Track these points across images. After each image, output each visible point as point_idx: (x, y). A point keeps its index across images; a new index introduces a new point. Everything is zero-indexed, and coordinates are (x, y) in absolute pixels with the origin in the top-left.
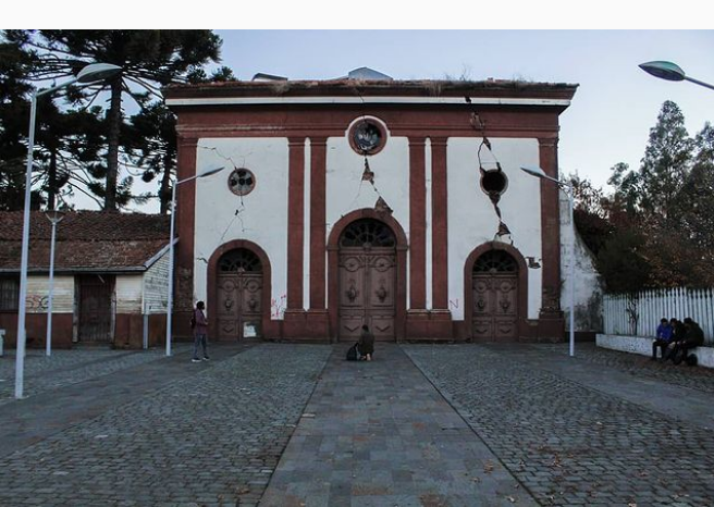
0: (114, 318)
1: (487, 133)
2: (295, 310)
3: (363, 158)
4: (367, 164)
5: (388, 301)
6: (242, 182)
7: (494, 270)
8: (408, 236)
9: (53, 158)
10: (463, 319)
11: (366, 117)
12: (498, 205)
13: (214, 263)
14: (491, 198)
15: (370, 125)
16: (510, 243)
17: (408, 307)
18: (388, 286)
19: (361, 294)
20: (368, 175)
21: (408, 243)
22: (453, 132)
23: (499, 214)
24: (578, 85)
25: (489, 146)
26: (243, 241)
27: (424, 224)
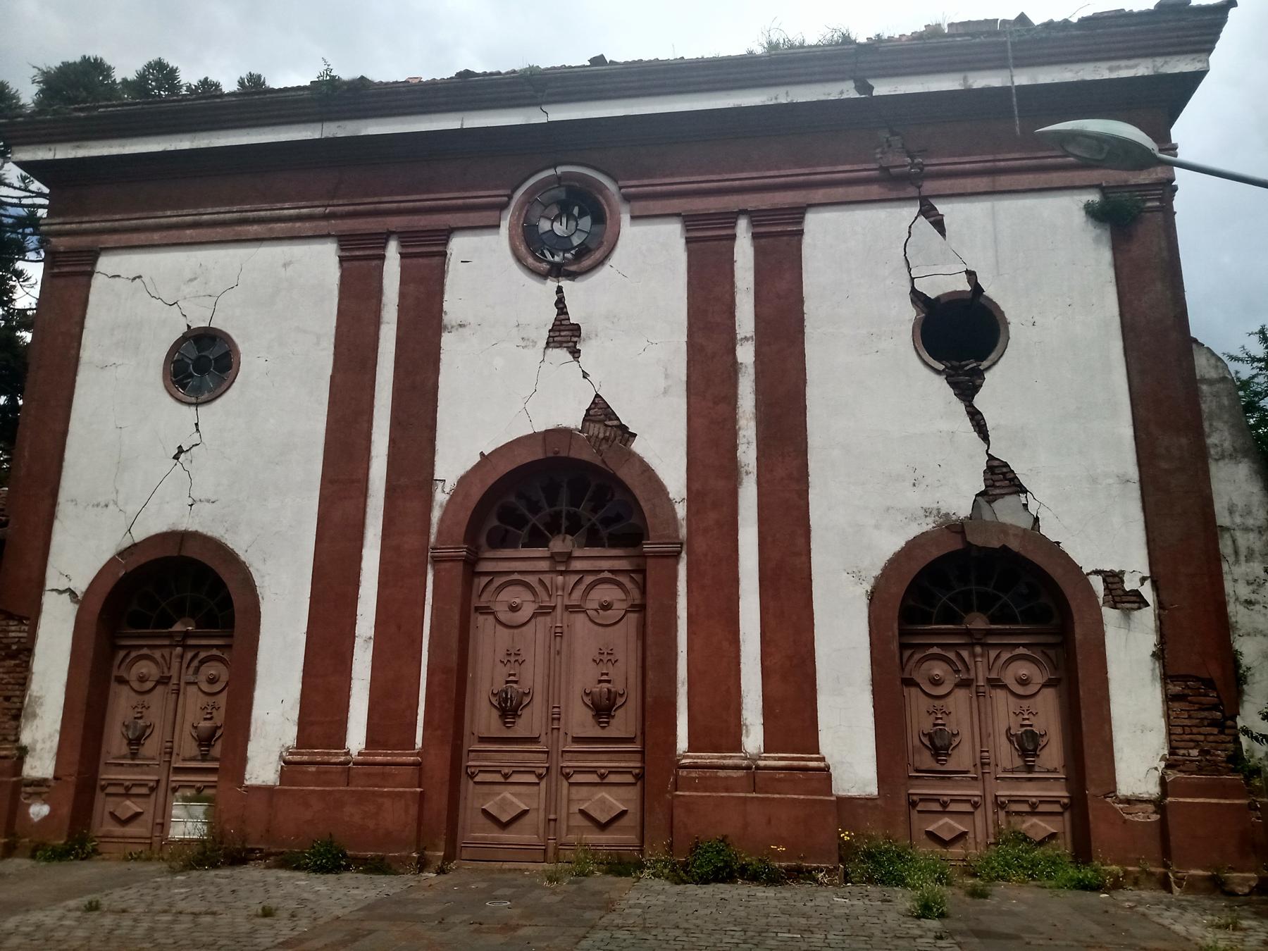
1: (929, 187)
2: (319, 754)
3: (551, 285)
4: (560, 304)
5: (624, 723)
6: (202, 366)
7: (978, 622)
8: (681, 511)
10: (872, 789)
11: (561, 170)
14: (953, 385)
15: (571, 191)
16: (1026, 523)
17: (682, 743)
18: (624, 674)
19: (538, 699)
21: (683, 532)
22: (819, 195)
23: (984, 435)
25: (939, 225)
27: (732, 473)
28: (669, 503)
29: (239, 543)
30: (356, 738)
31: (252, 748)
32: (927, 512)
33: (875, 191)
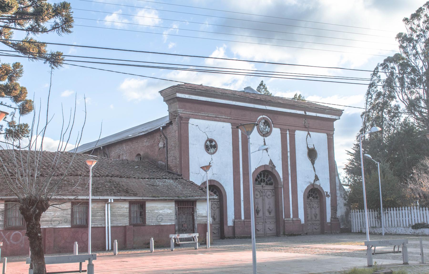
1: (309, 129)
6: (212, 146)
8: (282, 180)
14: (312, 163)
27: (288, 174)
28: (280, 179)
29: (222, 182)
30: (243, 218)
31: (228, 219)
32: (309, 182)
33: (304, 128)
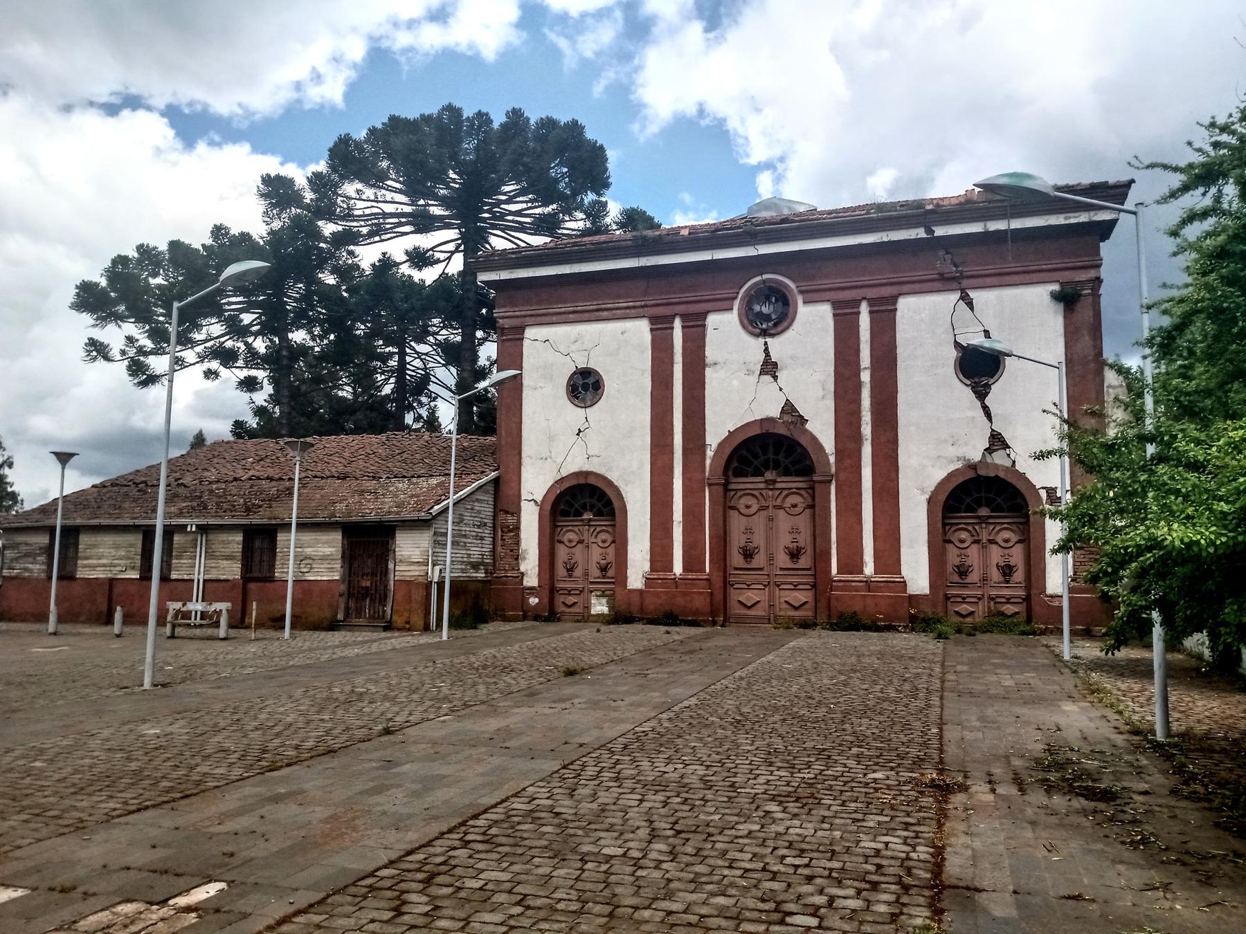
0: (392, 583)
1: (965, 283)
2: (662, 575)
3: (761, 340)
4: (766, 350)
5: (805, 561)
6: (586, 387)
7: (984, 512)
8: (832, 459)
9: (402, 354)
10: (927, 591)
11: (765, 276)
12: (988, 401)
13: (548, 507)
14: (975, 392)
15: (770, 288)
16: (1008, 463)
17: (834, 570)
18: (804, 539)
19: (762, 551)
20: (769, 368)
21: (833, 470)
22: (906, 288)
24: (1133, 181)
25: (970, 305)
26: (587, 474)
27: (858, 439)
28: (826, 455)
29: (613, 476)
30: (678, 568)
31: (629, 572)
32: (959, 459)
33: (937, 285)
